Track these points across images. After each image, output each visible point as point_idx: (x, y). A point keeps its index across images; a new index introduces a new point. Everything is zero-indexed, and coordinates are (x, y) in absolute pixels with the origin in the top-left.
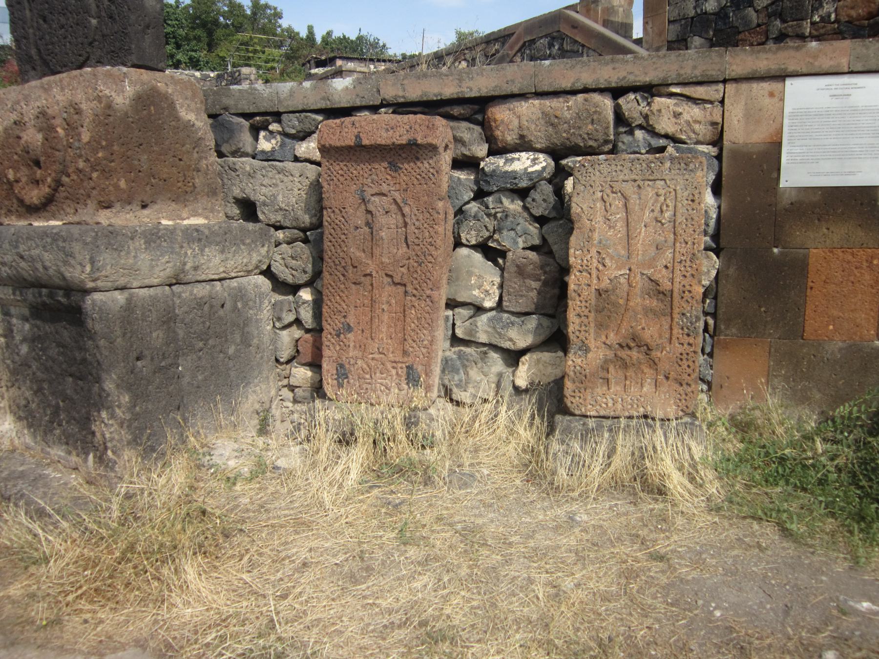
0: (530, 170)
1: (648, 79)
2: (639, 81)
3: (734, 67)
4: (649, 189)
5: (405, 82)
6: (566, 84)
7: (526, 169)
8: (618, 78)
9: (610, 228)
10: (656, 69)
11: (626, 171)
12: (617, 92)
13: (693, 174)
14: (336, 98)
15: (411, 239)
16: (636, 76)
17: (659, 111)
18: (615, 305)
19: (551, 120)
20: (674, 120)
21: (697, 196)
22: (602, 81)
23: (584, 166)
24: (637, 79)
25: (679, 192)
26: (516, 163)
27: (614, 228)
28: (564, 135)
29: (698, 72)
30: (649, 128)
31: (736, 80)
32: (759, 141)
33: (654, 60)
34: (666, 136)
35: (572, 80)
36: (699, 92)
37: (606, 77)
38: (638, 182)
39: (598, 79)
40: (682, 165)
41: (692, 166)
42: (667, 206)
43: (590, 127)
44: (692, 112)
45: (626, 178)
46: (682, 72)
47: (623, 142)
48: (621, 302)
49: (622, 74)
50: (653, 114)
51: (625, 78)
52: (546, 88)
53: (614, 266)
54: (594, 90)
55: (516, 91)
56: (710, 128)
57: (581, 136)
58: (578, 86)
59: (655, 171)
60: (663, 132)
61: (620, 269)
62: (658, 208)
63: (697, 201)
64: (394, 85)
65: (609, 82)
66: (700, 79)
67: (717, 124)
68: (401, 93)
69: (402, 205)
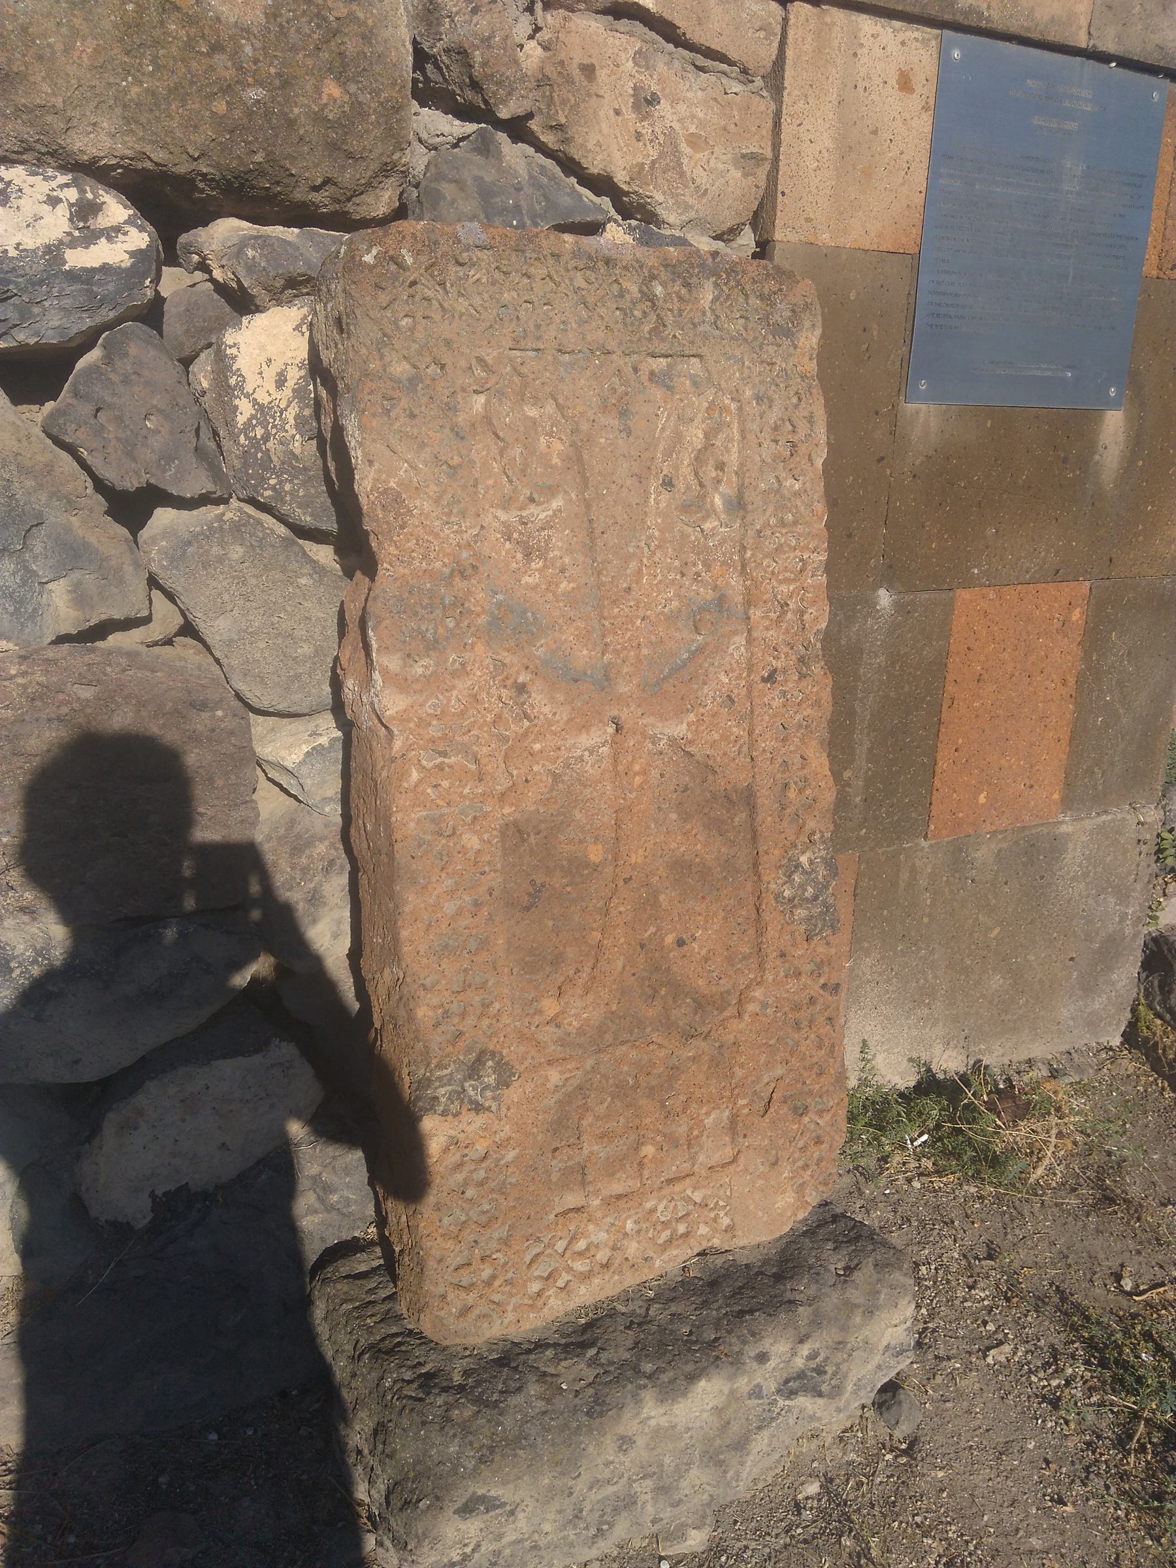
0: (77, 259)
4: (657, 393)
7: (54, 252)
9: (527, 555)
13: (787, 342)
17: (589, 71)
18: (578, 868)
20: (630, 115)
21: (803, 429)
23: (401, 266)
27: (543, 555)
28: (220, 107)
30: (548, 138)
34: (602, 185)
38: (617, 360)
40: (754, 302)
42: (721, 466)
43: (332, 89)
44: (690, 100)
45: (571, 340)
47: (460, 184)
48: (595, 854)
50: (569, 80)
57: (291, 123)
59: (669, 319)
60: (595, 167)
61: (585, 728)
62: (686, 470)
63: (803, 449)
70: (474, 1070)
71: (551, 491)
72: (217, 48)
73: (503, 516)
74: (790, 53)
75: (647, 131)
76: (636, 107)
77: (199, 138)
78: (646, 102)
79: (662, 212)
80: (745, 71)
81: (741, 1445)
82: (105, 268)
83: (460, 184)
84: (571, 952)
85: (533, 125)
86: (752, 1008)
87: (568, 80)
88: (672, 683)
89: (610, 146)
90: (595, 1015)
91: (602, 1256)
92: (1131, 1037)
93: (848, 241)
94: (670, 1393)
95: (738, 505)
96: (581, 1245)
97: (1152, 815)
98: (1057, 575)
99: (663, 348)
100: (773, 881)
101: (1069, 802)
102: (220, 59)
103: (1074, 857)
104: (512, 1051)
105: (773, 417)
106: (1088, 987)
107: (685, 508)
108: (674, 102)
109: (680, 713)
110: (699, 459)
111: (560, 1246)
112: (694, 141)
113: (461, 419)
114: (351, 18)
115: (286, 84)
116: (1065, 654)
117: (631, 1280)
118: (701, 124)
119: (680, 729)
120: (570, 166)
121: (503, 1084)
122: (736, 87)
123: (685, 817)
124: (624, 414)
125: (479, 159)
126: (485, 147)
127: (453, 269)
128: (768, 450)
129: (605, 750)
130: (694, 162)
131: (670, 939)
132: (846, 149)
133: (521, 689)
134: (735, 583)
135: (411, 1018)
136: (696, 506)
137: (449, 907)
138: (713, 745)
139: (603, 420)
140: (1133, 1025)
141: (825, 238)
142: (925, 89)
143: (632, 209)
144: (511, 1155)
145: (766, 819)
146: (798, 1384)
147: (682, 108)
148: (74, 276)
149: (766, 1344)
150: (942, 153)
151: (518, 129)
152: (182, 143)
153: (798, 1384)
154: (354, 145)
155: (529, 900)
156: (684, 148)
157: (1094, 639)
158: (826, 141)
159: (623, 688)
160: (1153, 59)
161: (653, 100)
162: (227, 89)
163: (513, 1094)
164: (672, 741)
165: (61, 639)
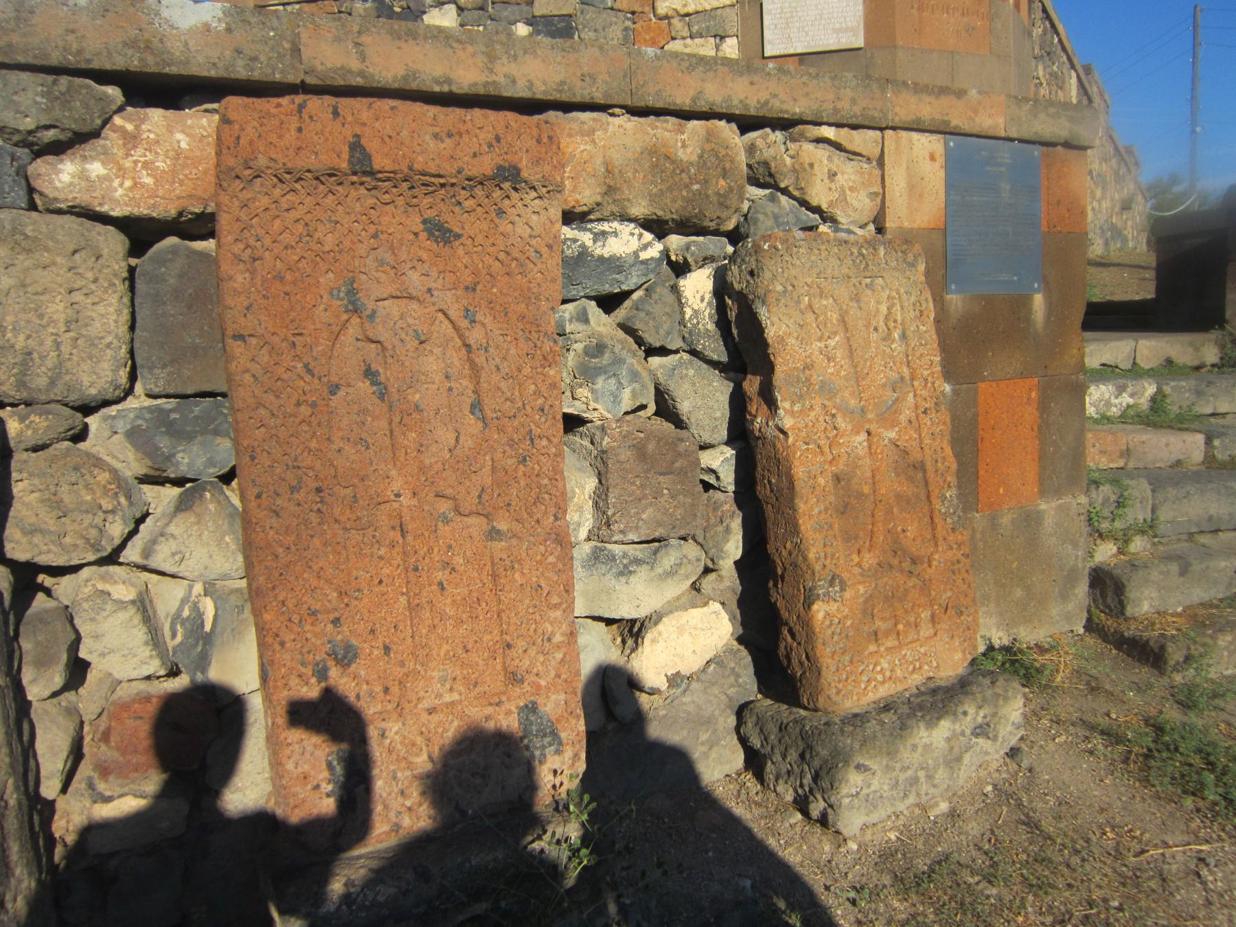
0: (644, 256)
1: (797, 110)
2: (787, 112)
3: (897, 109)
4: (869, 292)
5: (365, 39)
6: (683, 99)
7: (636, 254)
8: (758, 102)
10: (807, 94)
11: (834, 262)
12: (747, 124)
14: (175, 47)
15: (489, 403)
16: (782, 102)
17: (811, 165)
18: (860, 495)
19: (659, 160)
20: (827, 181)
22: (735, 102)
24: (784, 107)
25: (904, 297)
26: (611, 241)
29: (857, 110)
30: (796, 193)
31: (894, 128)
32: (924, 225)
33: (805, 79)
34: (817, 210)
35: (692, 93)
36: (863, 140)
37: (742, 97)
38: (854, 280)
39: (730, 98)
41: (910, 258)
42: (895, 321)
43: (722, 182)
44: (849, 172)
45: (836, 273)
46: (839, 106)
47: (765, 214)
49: (764, 96)
50: (805, 170)
51: (767, 102)
52: (651, 101)
53: (850, 428)
54: (720, 116)
55: (599, 98)
56: (868, 201)
57: (707, 196)
58: (703, 106)
60: (814, 203)
63: (925, 313)
64: (337, 39)
65: (746, 106)
66: (854, 121)
67: (876, 194)
68: (355, 65)
69: (464, 324)
70: (832, 584)
71: (835, 333)
72: (683, 171)
73: (819, 344)
74: (886, 150)
75: (833, 187)
76: (829, 177)
77: (676, 206)
78: (832, 175)
79: (840, 219)
80: (869, 159)
81: (959, 759)
82: (652, 259)
83: (765, 214)
84: (861, 534)
85: (791, 189)
86: (935, 563)
87: (802, 170)
88: (888, 416)
89: (819, 195)
90: (874, 561)
91: (888, 674)
92: (1090, 626)
93: (915, 225)
94: (931, 725)
95: (904, 336)
96: (878, 668)
97: (1083, 499)
98: (1022, 376)
99: (869, 274)
100: (937, 505)
101: (1043, 493)
102: (684, 175)
103: (1049, 522)
104: (845, 575)
105: (913, 299)
106: (1064, 597)
107: (884, 339)
108: (843, 174)
109: (892, 427)
110: (887, 318)
111: (871, 667)
112: (851, 189)
113: (802, 306)
114: (727, 155)
115: (706, 182)
116: (1030, 413)
117: (900, 688)
118: (854, 182)
119: (892, 434)
120: (804, 203)
121: (843, 590)
122: (866, 166)
123: (898, 475)
124: (858, 301)
125: (770, 204)
126: (772, 199)
127: (795, 250)
128: (912, 314)
129: (865, 444)
130: (852, 198)
131: (899, 529)
132: (911, 187)
133: (834, 416)
134: (906, 371)
135: (805, 559)
136: (887, 338)
137: (816, 511)
138: (907, 441)
139: (851, 304)
140: (1089, 620)
141: (906, 224)
142: (941, 160)
143: (826, 217)
144: (849, 623)
145: (931, 475)
146: (982, 730)
147: (846, 176)
148: (643, 262)
149: (966, 707)
150: (950, 186)
151: (785, 191)
152: (670, 209)
153: (982, 730)
154: (728, 203)
155: (843, 510)
156: (848, 192)
157: (1043, 407)
158: (903, 184)
159: (870, 416)
160: (1033, 138)
161: (835, 174)
162: (687, 186)
163: (848, 594)
164: (890, 440)
165: (627, 413)
